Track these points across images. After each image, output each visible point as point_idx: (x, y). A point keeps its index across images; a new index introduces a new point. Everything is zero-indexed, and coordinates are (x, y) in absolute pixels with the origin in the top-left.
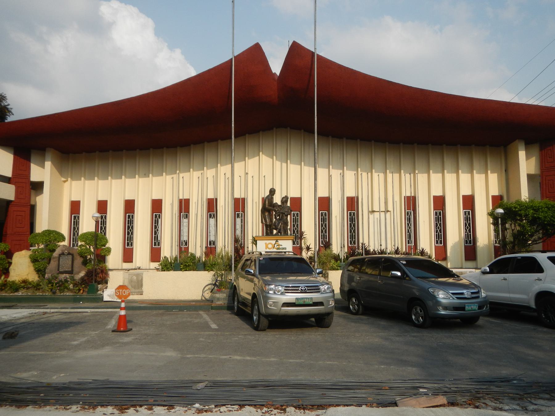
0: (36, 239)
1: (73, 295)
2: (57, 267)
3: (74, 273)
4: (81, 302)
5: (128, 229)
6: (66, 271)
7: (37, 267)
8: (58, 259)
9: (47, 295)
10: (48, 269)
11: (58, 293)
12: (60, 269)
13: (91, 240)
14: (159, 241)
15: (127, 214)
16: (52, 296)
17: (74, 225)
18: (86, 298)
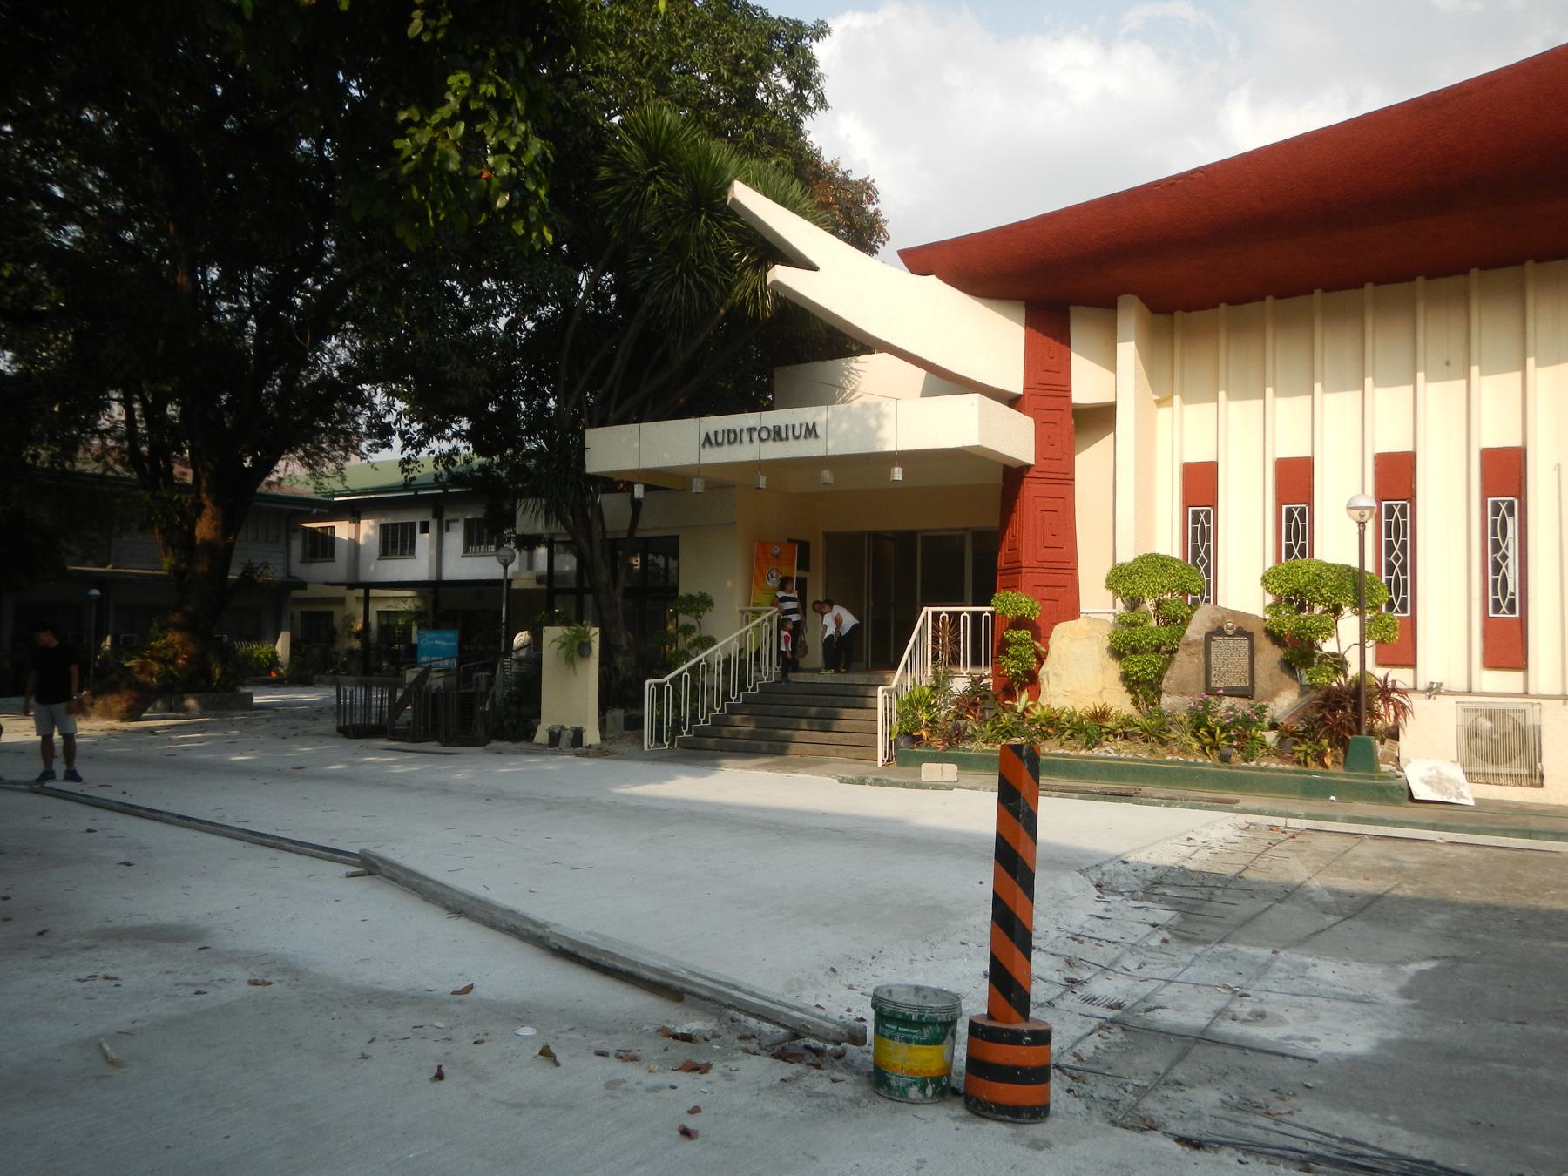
0: (1134, 582)
1: (1295, 772)
2: (1202, 675)
3: (1255, 697)
4: (1333, 798)
5: (1388, 554)
6: (1233, 688)
7: (1136, 669)
8: (1202, 647)
9: (1200, 765)
10: (1169, 679)
11: (1236, 758)
12: (1213, 679)
13: (1337, 587)
14: (1513, 594)
15: (1190, 509)
16: (1220, 767)
17: (1194, 539)
18: (1345, 783)
